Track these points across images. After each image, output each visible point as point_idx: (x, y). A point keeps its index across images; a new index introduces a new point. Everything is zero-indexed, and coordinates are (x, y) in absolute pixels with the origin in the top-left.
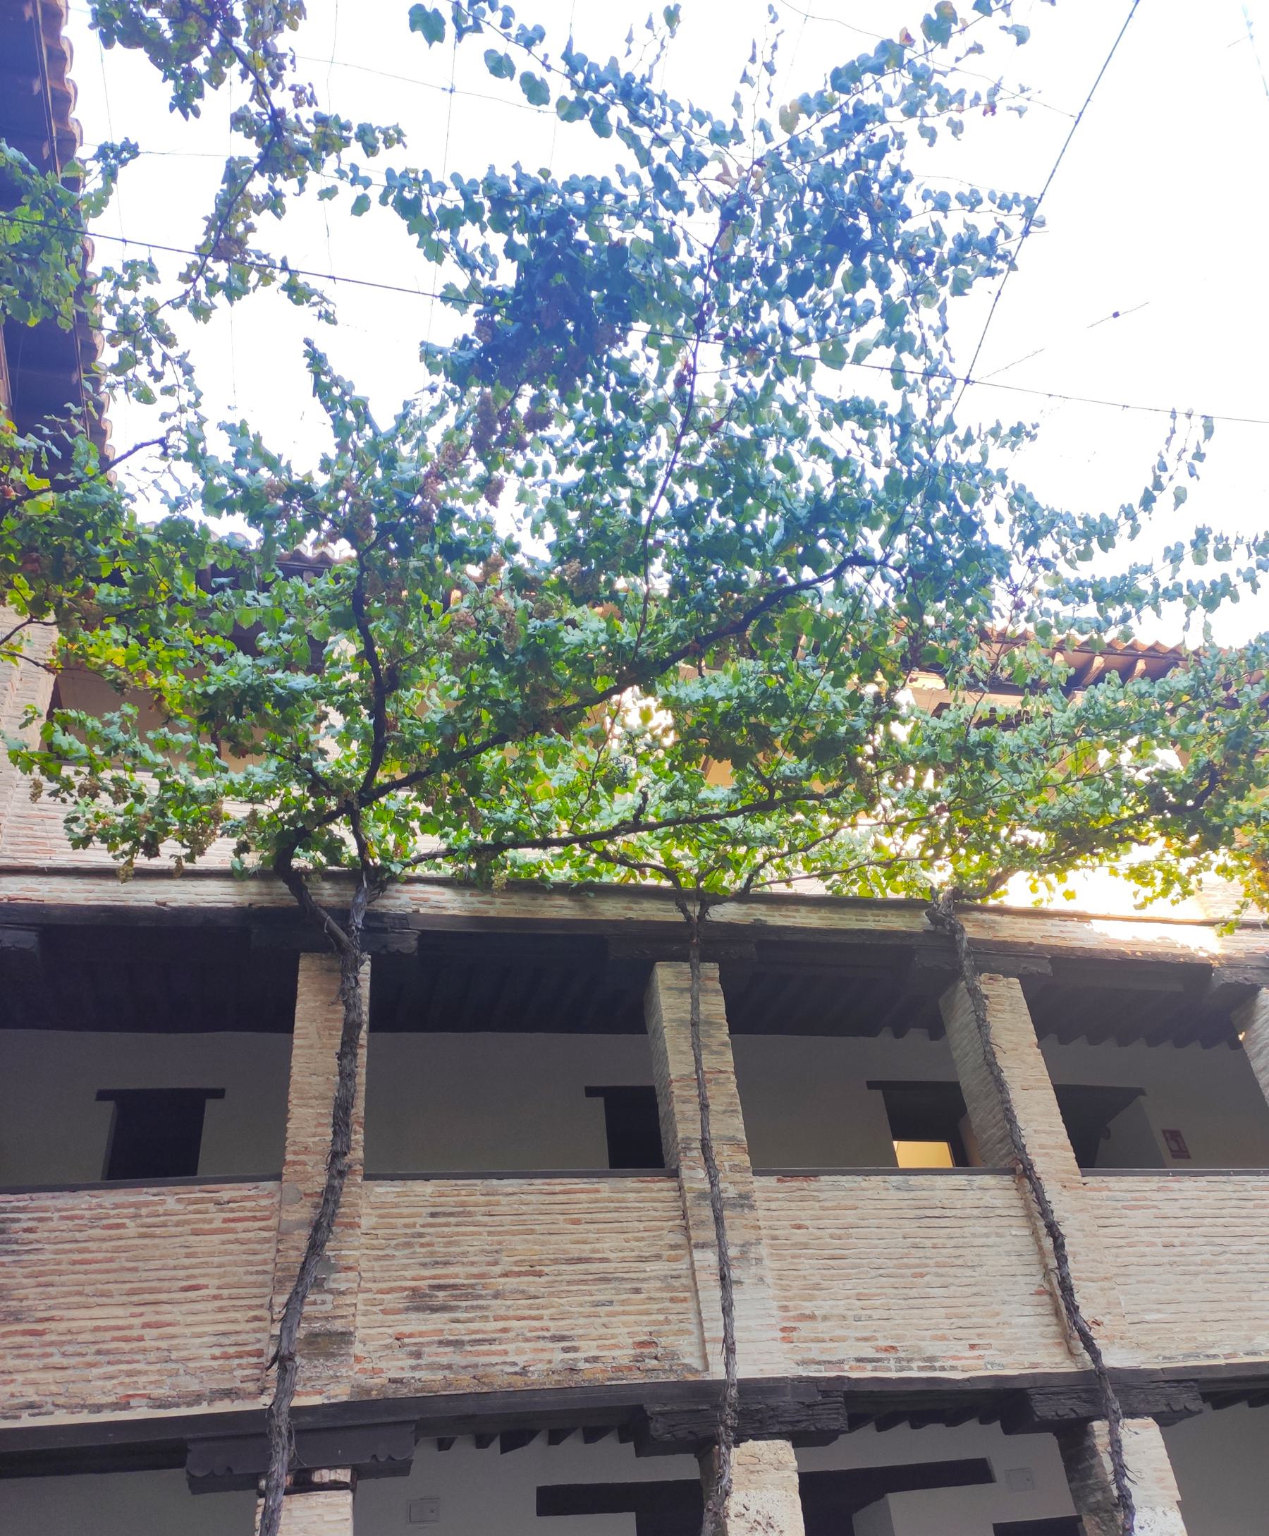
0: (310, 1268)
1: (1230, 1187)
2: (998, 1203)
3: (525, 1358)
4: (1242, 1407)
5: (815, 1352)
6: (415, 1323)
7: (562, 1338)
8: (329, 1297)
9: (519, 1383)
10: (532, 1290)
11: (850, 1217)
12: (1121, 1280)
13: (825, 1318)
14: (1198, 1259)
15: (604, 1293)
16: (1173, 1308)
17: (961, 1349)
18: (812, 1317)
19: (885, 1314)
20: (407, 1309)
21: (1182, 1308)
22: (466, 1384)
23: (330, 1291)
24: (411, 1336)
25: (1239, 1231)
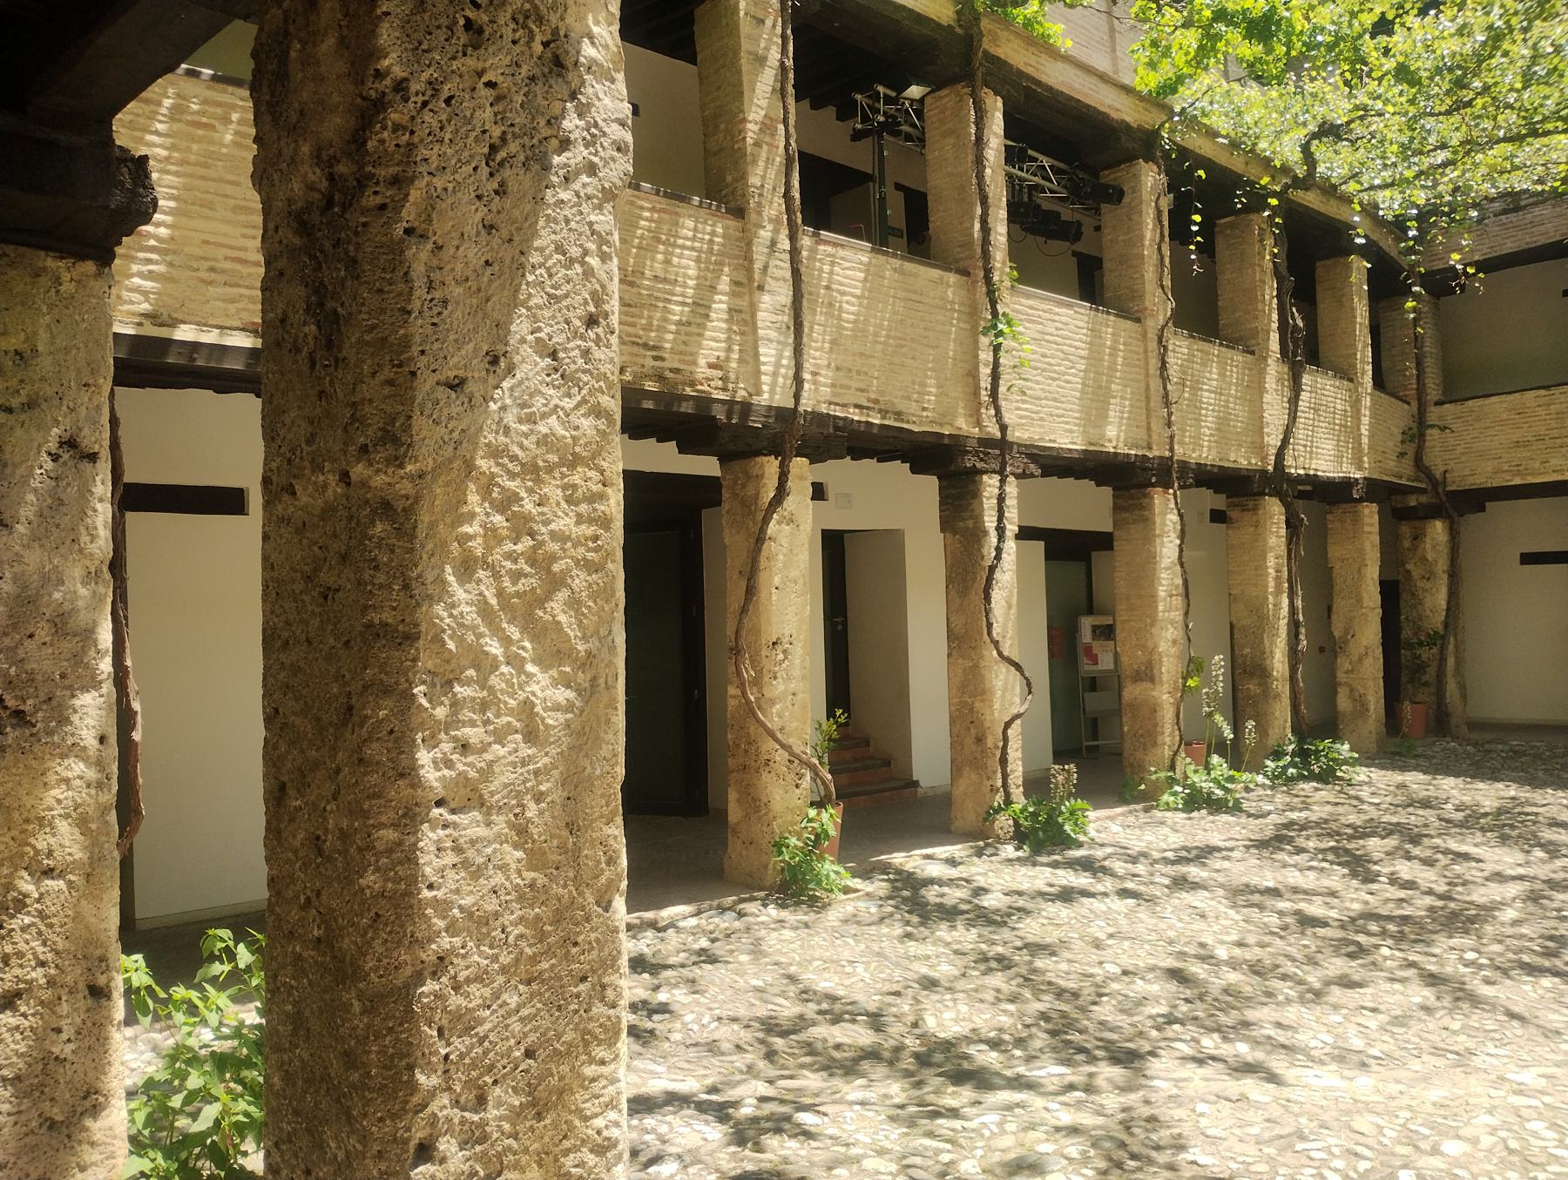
4: (900, 469)
7: (654, 348)
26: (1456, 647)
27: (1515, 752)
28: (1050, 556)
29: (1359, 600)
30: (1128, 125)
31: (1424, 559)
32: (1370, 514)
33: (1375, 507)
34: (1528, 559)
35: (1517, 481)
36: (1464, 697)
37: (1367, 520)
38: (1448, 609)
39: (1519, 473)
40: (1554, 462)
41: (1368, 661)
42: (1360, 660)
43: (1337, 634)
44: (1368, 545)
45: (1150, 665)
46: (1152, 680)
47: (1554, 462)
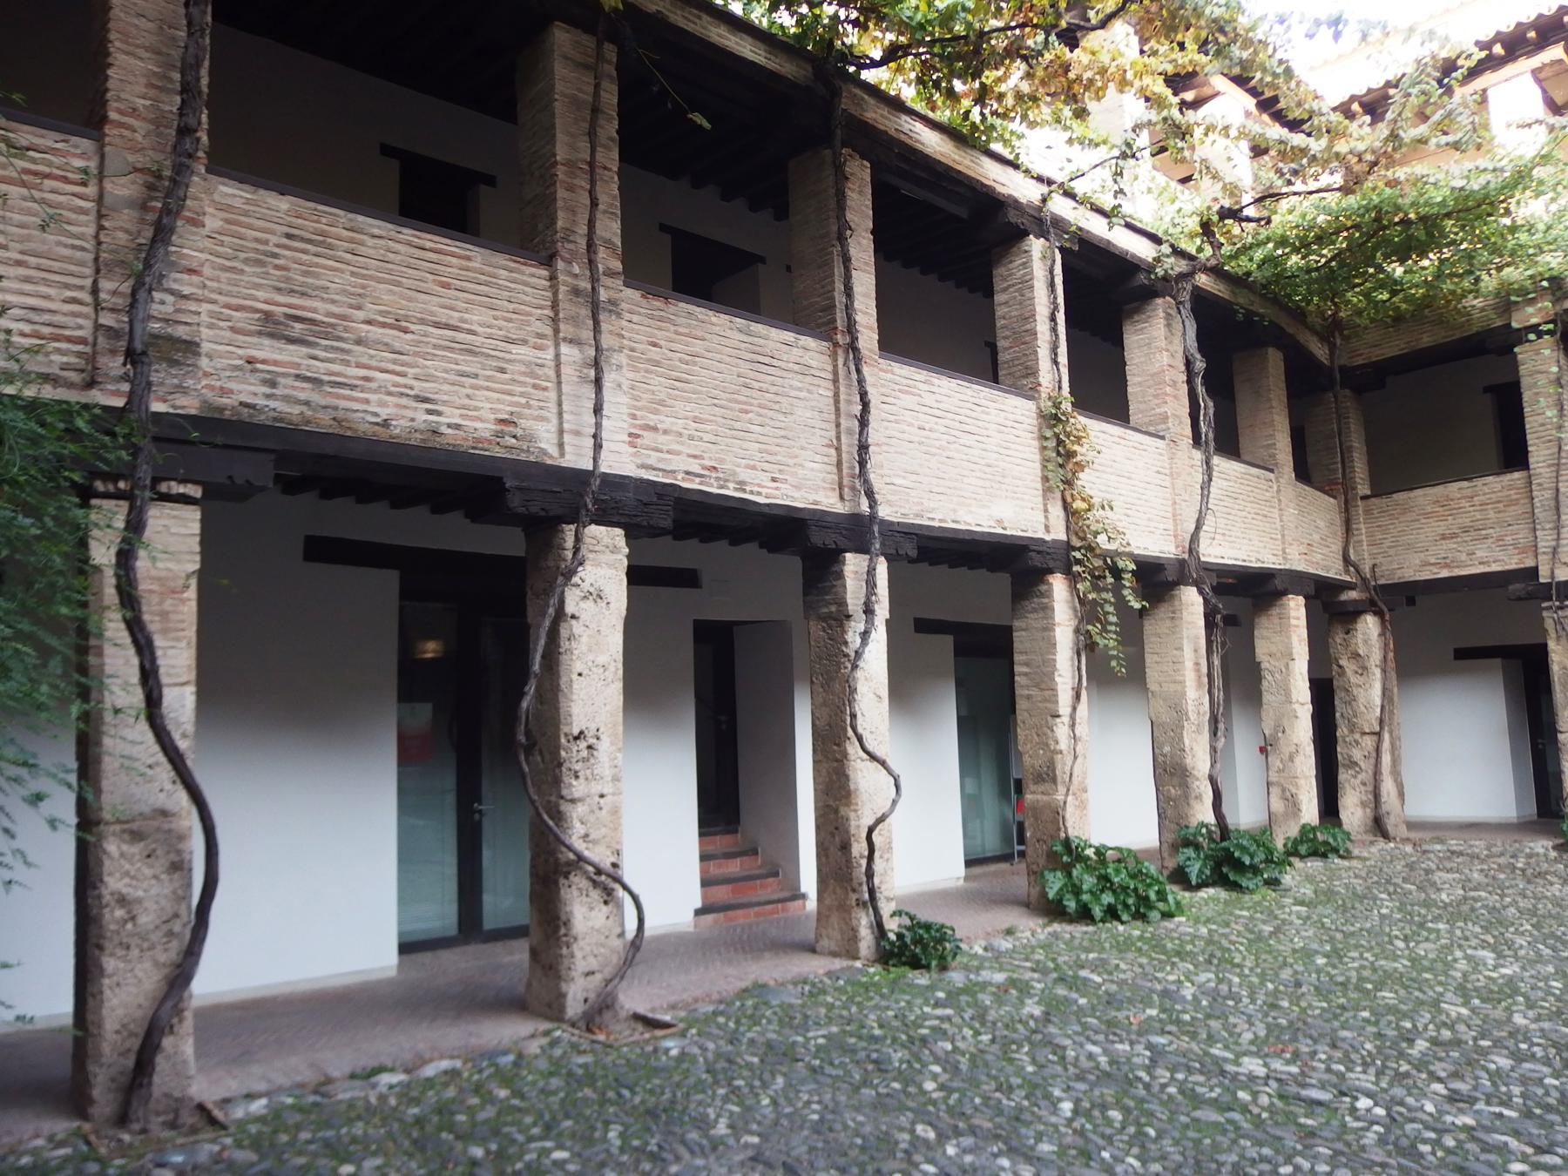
0: (148, 262)
1: (969, 392)
2: (814, 363)
3: (389, 411)
5: (653, 458)
6: (267, 350)
7: (426, 400)
8: (170, 299)
9: (383, 434)
10: (397, 345)
11: (698, 346)
12: (885, 448)
13: (665, 432)
14: (937, 443)
15: (470, 364)
16: (914, 477)
17: (764, 479)
18: (655, 429)
19: (713, 439)
20: (260, 333)
21: (919, 478)
22: (324, 422)
23: (172, 292)
24: (263, 362)
25: (967, 428)
26: (1393, 745)
27: (1453, 852)
28: (959, 651)
29: (1288, 694)
30: (1016, 201)
31: (1356, 656)
32: (1296, 607)
33: (1301, 600)
34: (1463, 654)
35: (1445, 574)
36: (1401, 795)
37: (1293, 613)
38: (1383, 707)
39: (1447, 566)
40: (1479, 554)
41: (1299, 760)
42: (1291, 759)
43: (1267, 732)
44: (1295, 639)
45: (1051, 766)
46: (1054, 780)
47: (1479, 554)
